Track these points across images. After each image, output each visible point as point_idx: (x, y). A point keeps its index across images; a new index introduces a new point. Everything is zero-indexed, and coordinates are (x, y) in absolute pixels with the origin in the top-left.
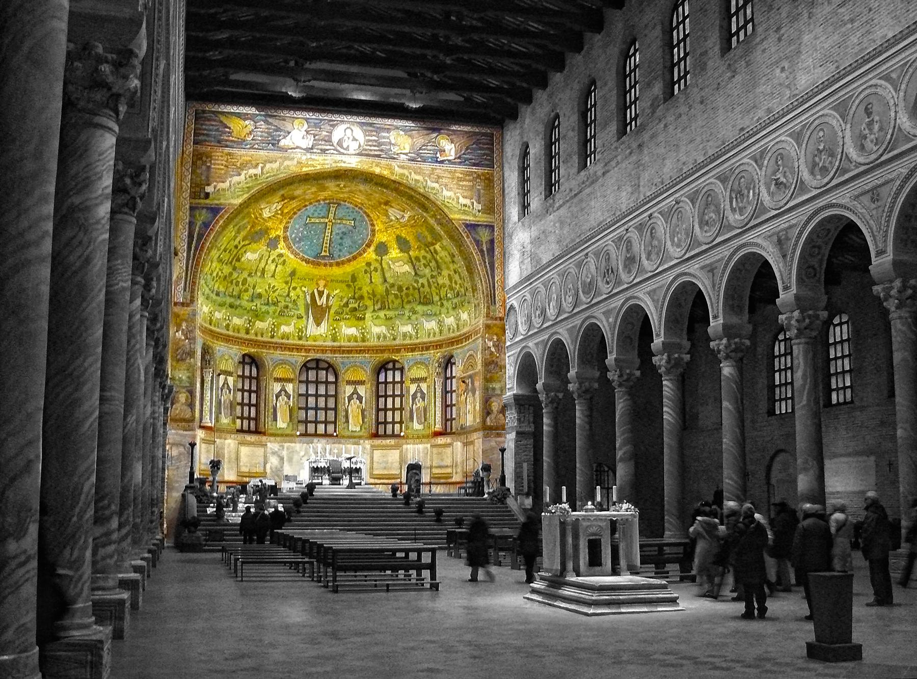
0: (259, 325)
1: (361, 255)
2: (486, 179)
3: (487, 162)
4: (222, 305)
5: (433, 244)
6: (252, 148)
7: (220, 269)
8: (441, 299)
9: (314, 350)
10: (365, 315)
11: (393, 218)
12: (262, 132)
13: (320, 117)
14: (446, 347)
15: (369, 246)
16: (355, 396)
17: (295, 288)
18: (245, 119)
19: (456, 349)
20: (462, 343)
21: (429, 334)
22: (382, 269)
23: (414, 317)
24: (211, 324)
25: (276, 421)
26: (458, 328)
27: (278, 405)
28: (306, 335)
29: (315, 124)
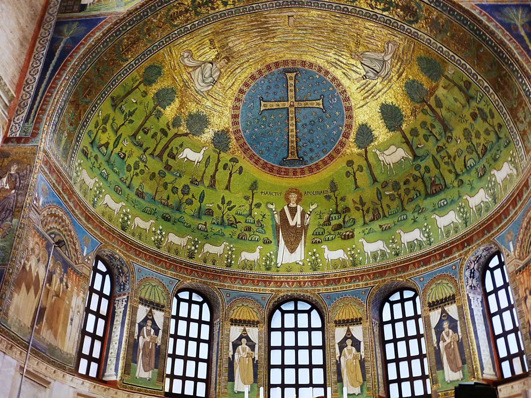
0: (209, 248)
1: (337, 151)
4: (148, 213)
5: (433, 90)
7: (139, 158)
8: (457, 175)
9: (288, 282)
10: (353, 232)
11: (371, 74)
14: (479, 238)
15: (346, 136)
16: (349, 342)
17: (258, 206)
19: (496, 233)
20: (509, 215)
21: (448, 233)
22: (369, 166)
23: (420, 218)
24: (123, 229)
25: (233, 380)
26: (495, 200)
28: (276, 264)
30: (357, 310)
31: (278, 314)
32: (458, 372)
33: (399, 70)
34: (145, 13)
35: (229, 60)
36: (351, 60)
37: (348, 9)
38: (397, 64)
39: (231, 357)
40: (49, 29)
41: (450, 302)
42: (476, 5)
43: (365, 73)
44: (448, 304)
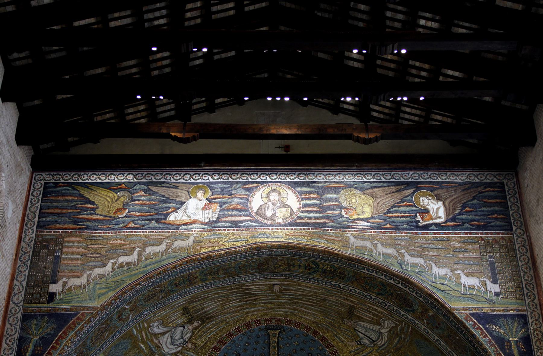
2: (500, 246)
3: (498, 223)
6: (126, 228)
11: (366, 341)
12: (141, 205)
13: (231, 180)
18: (116, 191)
29: (222, 189)
33: (396, 344)
34: (119, 304)
35: (203, 322)
36: (343, 325)
37: (340, 286)
38: (395, 339)
40: (16, 324)
42: (470, 314)
43: (359, 339)
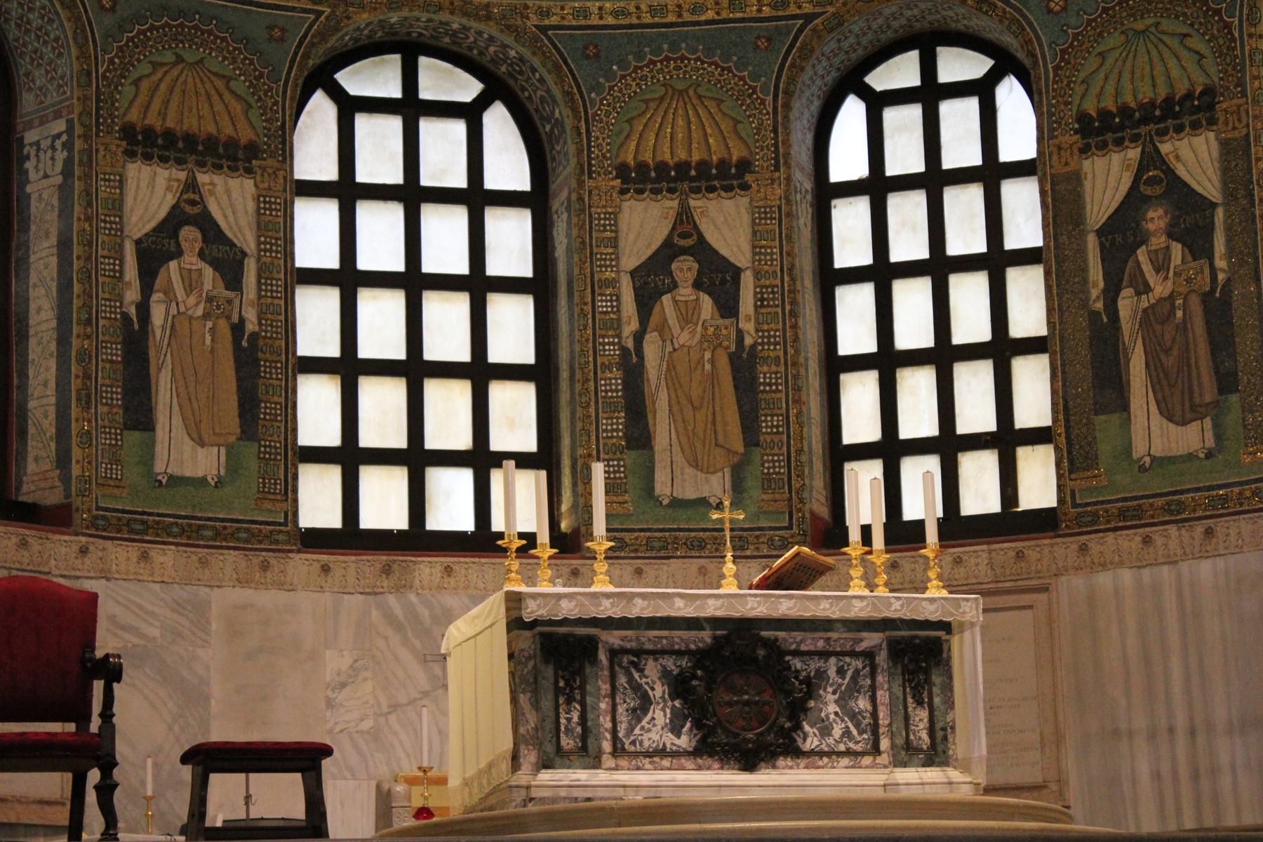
16: (685, 268)
27: (158, 315)
30: (725, 125)
31: (321, 110)
32: (1196, 426)
39: (132, 311)
41: (1186, 120)
44: (1179, 129)
